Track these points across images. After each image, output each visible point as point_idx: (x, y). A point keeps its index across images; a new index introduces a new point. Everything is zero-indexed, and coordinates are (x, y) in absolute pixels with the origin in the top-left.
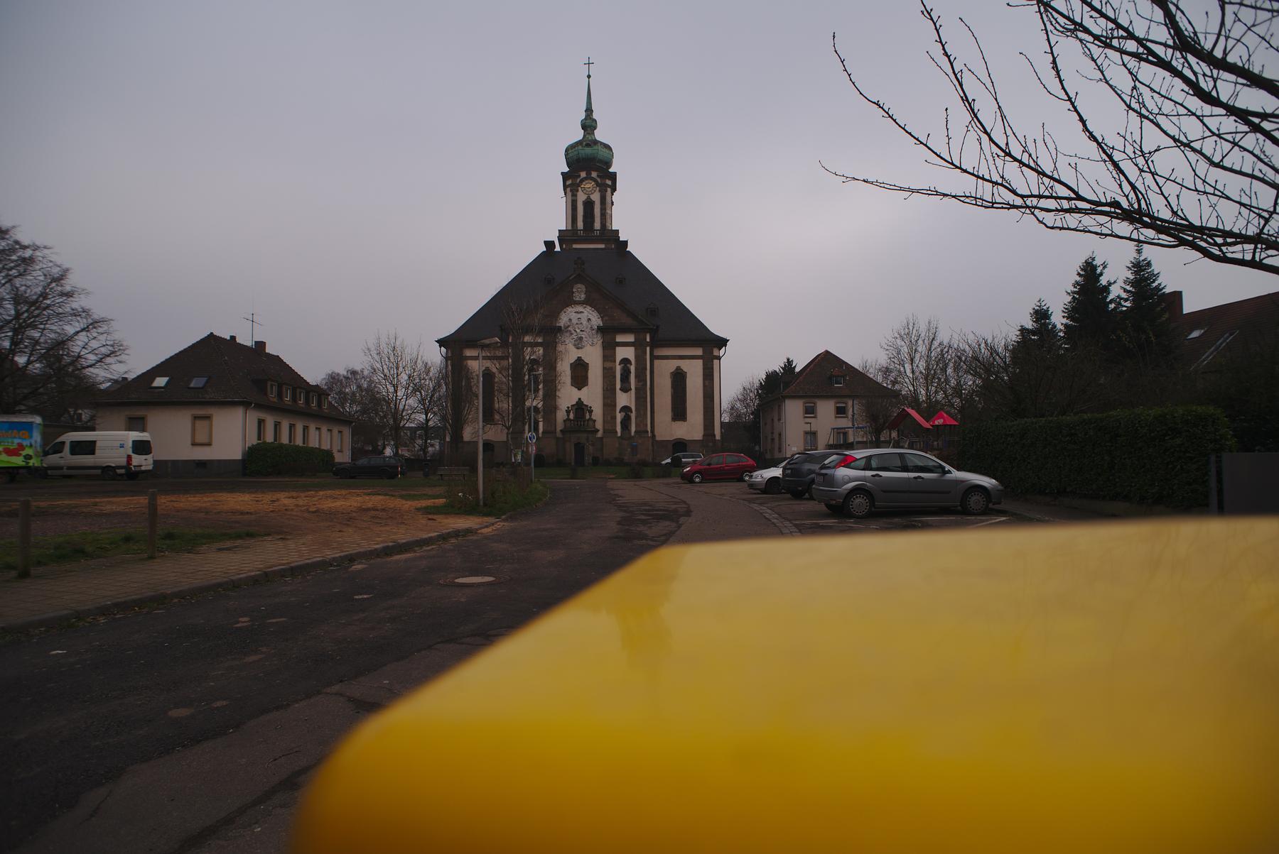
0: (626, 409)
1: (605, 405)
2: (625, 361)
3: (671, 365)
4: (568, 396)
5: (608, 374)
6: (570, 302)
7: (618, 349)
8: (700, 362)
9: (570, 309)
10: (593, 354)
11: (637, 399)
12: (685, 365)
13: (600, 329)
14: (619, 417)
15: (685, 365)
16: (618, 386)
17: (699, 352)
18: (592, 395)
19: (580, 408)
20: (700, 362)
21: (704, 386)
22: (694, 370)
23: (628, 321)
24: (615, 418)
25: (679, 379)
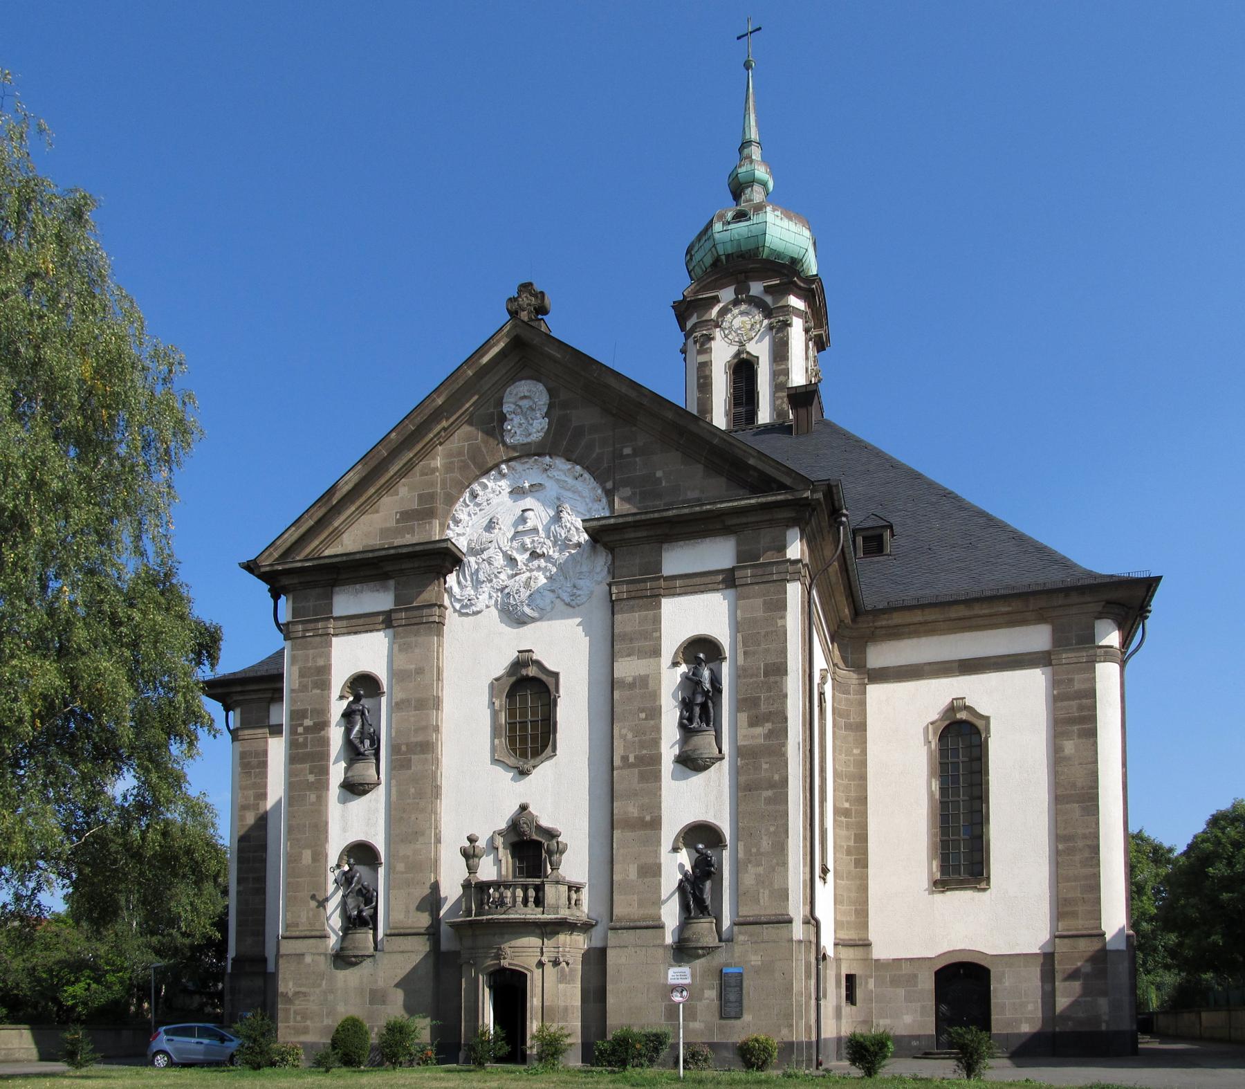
0: (701, 836)
2: (701, 650)
3: (928, 699)
4: (475, 796)
5: (619, 702)
7: (671, 607)
12: (982, 693)
14: (675, 864)
15: (982, 693)
19: (530, 847)
21: (1057, 759)
22: (1014, 708)
23: (700, 489)
24: (652, 871)
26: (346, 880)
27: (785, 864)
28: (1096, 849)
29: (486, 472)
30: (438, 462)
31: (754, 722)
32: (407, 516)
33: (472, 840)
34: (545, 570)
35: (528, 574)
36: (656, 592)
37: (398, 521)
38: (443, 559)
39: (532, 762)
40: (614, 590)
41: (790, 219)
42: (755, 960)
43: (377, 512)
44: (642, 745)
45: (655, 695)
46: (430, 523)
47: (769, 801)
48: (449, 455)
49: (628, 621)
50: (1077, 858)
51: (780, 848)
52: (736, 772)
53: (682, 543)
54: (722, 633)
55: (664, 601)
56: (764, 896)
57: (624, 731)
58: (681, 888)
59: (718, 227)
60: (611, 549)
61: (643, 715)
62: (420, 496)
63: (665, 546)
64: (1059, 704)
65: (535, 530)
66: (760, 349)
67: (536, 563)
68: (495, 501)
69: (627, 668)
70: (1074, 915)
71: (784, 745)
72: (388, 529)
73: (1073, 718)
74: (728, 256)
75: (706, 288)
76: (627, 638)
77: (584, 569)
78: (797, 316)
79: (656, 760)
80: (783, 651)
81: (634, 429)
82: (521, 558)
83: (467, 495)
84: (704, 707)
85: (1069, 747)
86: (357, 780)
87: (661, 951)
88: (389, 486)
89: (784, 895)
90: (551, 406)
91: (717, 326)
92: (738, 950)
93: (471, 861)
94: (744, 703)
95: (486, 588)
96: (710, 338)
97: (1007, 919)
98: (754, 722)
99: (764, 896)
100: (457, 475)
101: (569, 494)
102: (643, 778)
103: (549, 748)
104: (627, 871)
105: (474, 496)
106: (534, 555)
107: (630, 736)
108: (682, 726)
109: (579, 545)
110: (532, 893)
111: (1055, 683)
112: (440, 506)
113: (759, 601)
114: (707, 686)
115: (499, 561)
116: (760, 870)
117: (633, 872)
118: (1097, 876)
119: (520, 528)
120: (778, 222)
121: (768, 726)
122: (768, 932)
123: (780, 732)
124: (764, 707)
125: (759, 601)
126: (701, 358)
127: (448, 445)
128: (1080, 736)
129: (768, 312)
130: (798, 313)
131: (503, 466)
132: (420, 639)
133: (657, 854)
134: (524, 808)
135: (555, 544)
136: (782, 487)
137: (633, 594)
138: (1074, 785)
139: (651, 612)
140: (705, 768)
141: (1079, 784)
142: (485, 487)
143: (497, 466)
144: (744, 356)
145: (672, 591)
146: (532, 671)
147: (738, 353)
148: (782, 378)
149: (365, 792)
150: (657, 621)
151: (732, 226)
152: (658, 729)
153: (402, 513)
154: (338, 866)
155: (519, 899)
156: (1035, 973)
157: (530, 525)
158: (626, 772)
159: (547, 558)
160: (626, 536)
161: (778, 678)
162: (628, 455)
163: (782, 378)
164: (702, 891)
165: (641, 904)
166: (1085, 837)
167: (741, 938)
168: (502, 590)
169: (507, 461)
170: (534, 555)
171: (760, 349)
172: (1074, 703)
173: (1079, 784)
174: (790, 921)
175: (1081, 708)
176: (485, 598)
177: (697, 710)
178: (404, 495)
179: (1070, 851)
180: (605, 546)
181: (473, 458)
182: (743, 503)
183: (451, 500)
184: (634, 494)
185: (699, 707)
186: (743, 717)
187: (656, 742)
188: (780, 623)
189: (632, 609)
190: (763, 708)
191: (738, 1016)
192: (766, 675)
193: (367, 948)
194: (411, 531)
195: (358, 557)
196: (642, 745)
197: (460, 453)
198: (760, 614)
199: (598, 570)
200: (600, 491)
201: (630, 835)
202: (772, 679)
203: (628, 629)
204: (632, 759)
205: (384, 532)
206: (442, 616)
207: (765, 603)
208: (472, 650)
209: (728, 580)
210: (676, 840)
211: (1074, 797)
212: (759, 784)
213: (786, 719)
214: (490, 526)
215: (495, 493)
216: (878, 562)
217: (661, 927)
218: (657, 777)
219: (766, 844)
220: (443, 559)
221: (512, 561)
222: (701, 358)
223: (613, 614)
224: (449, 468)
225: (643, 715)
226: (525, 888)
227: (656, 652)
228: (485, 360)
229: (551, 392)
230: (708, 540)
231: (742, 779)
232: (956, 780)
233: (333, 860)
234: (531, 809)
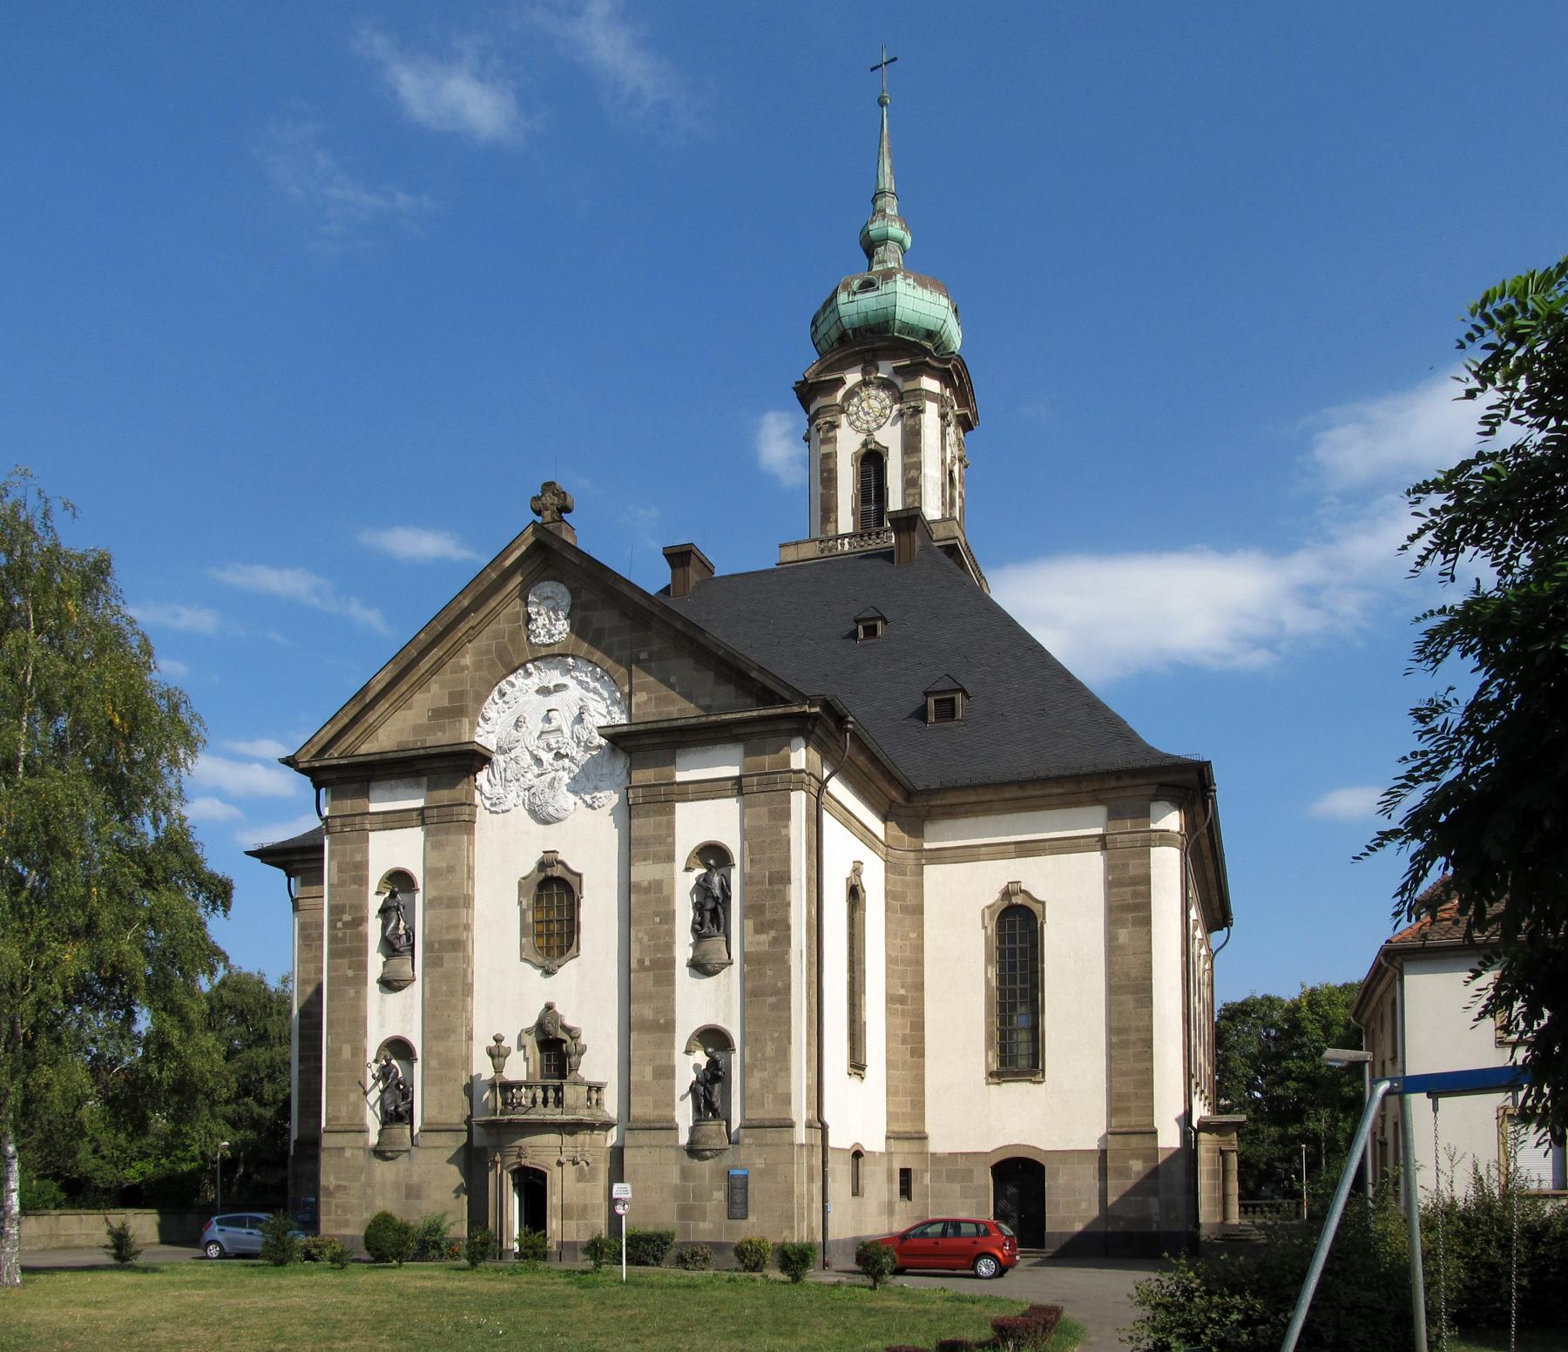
0: (712, 1038)
1: (628, 1026)
2: (712, 855)
6: (510, 661)
7: (684, 813)
8: (1094, 862)
9: (517, 679)
10: (590, 840)
11: (750, 995)
13: (618, 740)
14: (688, 1066)
16: (683, 949)
17: (1092, 822)
18: (587, 993)
19: (555, 1045)
20: (1094, 862)
21: (1112, 948)
24: (666, 1073)
25: (1017, 931)
26: (385, 1073)
27: (787, 1069)
28: (1148, 1043)
29: (514, 670)
30: (467, 660)
31: (760, 929)
32: (437, 713)
33: (498, 1039)
34: (570, 771)
35: (553, 774)
37: (430, 719)
38: (472, 760)
39: (557, 962)
40: (631, 795)
41: (924, 286)
42: (759, 1163)
43: (410, 708)
44: (657, 949)
45: (669, 900)
47: (773, 1007)
49: (644, 826)
50: (1131, 1051)
51: (783, 1054)
52: (744, 977)
54: (732, 841)
55: (680, 808)
56: (769, 1099)
57: (640, 935)
58: (693, 1090)
59: (843, 297)
60: (629, 752)
61: (657, 920)
62: (451, 695)
64: (1114, 890)
65: (559, 730)
66: (890, 437)
68: (521, 700)
69: (643, 872)
70: (1127, 1110)
71: (787, 952)
72: (421, 726)
73: (1128, 905)
74: (855, 330)
75: (830, 368)
76: (645, 842)
77: (605, 771)
78: (932, 400)
79: (670, 964)
80: (787, 860)
82: (547, 757)
83: (495, 693)
84: (714, 911)
85: (1123, 935)
86: (392, 976)
87: (673, 1152)
88: (420, 684)
89: (786, 1100)
90: (573, 607)
91: (843, 411)
92: (743, 1152)
93: (499, 1061)
94: (748, 910)
95: (514, 786)
96: (834, 426)
97: (1060, 1114)
98: (760, 929)
99: (769, 1099)
100: (485, 673)
101: (591, 695)
102: (657, 982)
103: (574, 948)
104: (643, 1073)
105: (502, 694)
107: (646, 939)
108: (694, 930)
109: (600, 747)
110: (551, 1094)
111: (1110, 868)
112: (471, 705)
113: (764, 810)
114: (717, 892)
115: (528, 760)
116: (765, 1074)
117: (648, 1074)
118: (1150, 1071)
119: (547, 727)
120: (910, 291)
121: (773, 933)
122: (771, 1135)
123: (784, 939)
124: (769, 915)
125: (764, 810)
126: (825, 449)
127: (476, 643)
128: (1134, 924)
129: (899, 397)
130: (932, 396)
131: (529, 666)
132: (452, 838)
133: (671, 1056)
134: (549, 1007)
135: (578, 745)
136: (785, 702)
138: (1128, 974)
140: (715, 973)
141: (1133, 975)
142: (513, 685)
144: (872, 446)
146: (557, 871)
147: (865, 444)
148: (913, 473)
149: (400, 989)
150: (671, 827)
151: (858, 297)
152: (671, 934)
154: (376, 1061)
155: (539, 1100)
156: (1092, 1168)
157: (554, 724)
158: (643, 975)
159: (572, 759)
161: (780, 887)
163: (913, 473)
164: (711, 1093)
165: (655, 1106)
166: (1138, 1030)
167: (747, 1141)
168: (529, 789)
169: (533, 661)
170: (559, 756)
171: (890, 437)
172: (1129, 889)
173: (1133, 975)
174: (791, 1126)
175: (1135, 895)
176: (513, 797)
177: (708, 915)
178: (433, 694)
179: (1124, 1045)
180: (623, 749)
181: (501, 657)
182: (746, 714)
183: (481, 699)
184: (650, 699)
185: (711, 912)
186: (749, 923)
187: (670, 946)
188: (784, 832)
189: (647, 815)
190: (768, 915)
191: (745, 1217)
192: (771, 883)
193: (402, 1144)
194: (442, 728)
196: (657, 949)
197: (488, 652)
198: (765, 822)
201: (646, 1037)
202: (776, 887)
203: (644, 833)
204: (647, 963)
205: (417, 729)
206: (473, 814)
207: (770, 811)
208: (502, 851)
209: (738, 787)
210: (689, 1043)
211: (1129, 988)
212: (765, 992)
213: (789, 927)
214: (518, 725)
215: (523, 688)
216: (947, 729)
217: (675, 1128)
218: (670, 980)
219: (770, 1049)
220: (472, 760)
221: (538, 761)
222: (825, 449)
224: (478, 666)
225: (657, 920)
226: (545, 1089)
227: (670, 858)
228: (508, 563)
229: (574, 593)
231: (749, 985)
232: (1012, 967)
233: (371, 1054)
234: (557, 1008)
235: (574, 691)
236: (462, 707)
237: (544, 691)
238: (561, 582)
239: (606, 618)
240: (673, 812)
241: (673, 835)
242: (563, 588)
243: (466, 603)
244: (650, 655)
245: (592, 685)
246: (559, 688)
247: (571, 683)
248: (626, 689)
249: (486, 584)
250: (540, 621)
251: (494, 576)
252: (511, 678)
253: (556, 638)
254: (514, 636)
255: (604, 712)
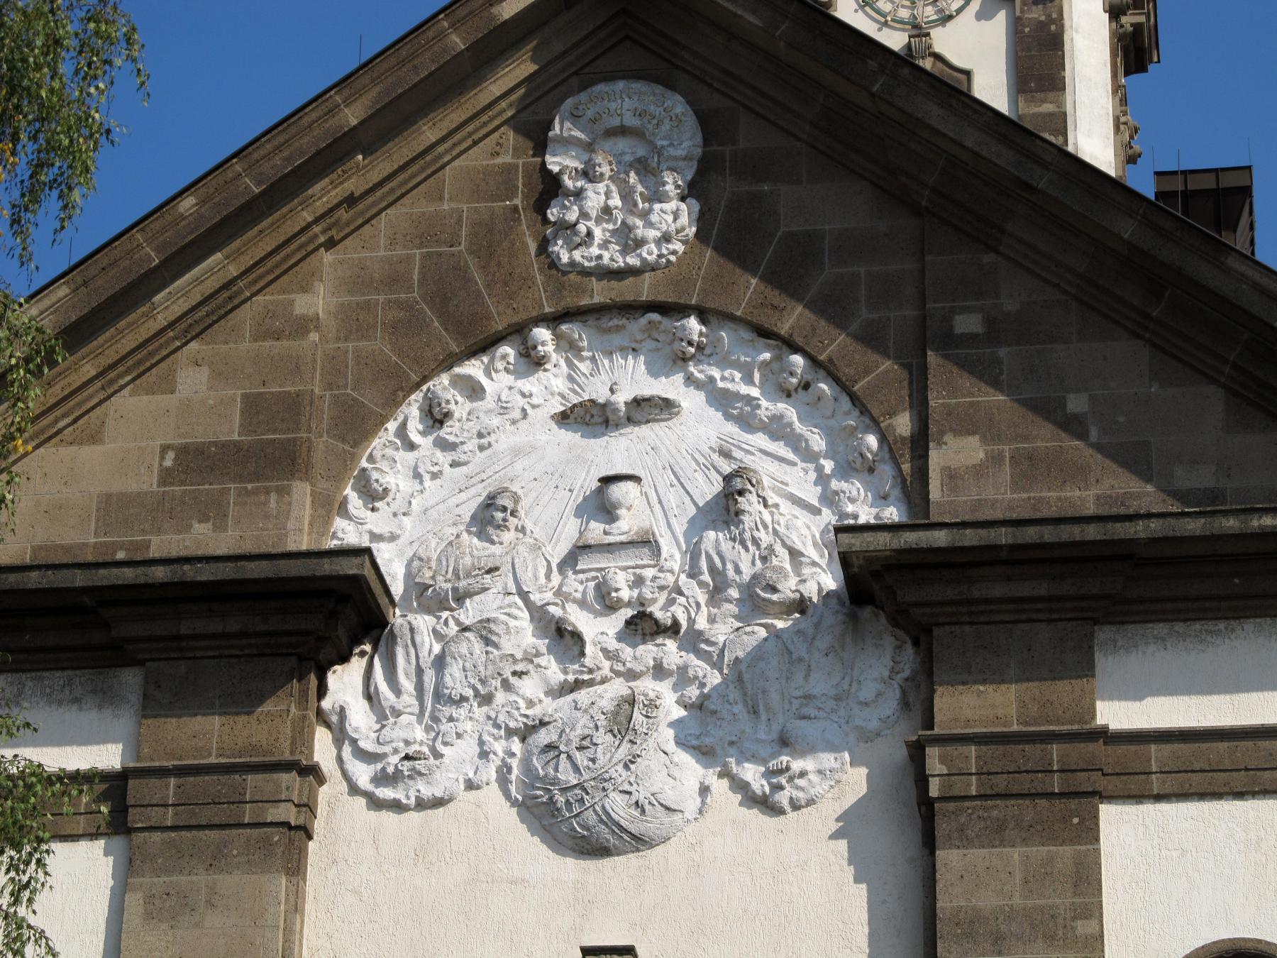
6: (488, 298)
7: (1136, 841)
9: (495, 375)
29: (484, 346)
30: (318, 301)
32: (195, 462)
34: (683, 677)
35: (618, 688)
36: (1083, 781)
37: (166, 477)
38: (337, 610)
40: (935, 761)
43: (95, 438)
46: (283, 492)
48: (359, 281)
53: (1161, 628)
55: (1111, 816)
60: (918, 632)
62: (252, 405)
63: (1103, 634)
65: (646, 542)
67: (647, 652)
68: (504, 441)
72: (126, 500)
77: (820, 684)
81: (988, 258)
82: (599, 631)
83: (412, 410)
88: (145, 363)
95: (470, 720)
100: (380, 345)
101: (761, 440)
105: (436, 417)
106: (642, 626)
109: (801, 605)
112: (322, 445)
115: (522, 635)
119: (596, 530)
127: (351, 250)
131: (542, 334)
132: (228, 882)
135: (716, 593)
137: (1001, 783)
139: (1067, 851)
142: (474, 391)
143: (518, 332)
145: (1134, 784)
150: (1086, 880)
153: (184, 452)
157: (626, 525)
159: (694, 641)
160: (977, 592)
162: (971, 339)
168: (525, 733)
169: (553, 321)
170: (642, 626)
176: (464, 754)
178: (196, 395)
183: (358, 426)
184: (995, 459)
189: (997, 834)
194: (214, 512)
195: (34, 580)
197: (394, 279)
199: (867, 692)
200: (872, 441)
203: (987, 901)
205: (114, 507)
206: (309, 807)
214: (490, 515)
220: (337, 610)
221: (564, 639)
223: (929, 843)
224: (354, 322)
229: (705, 120)
230: (1249, 625)
235: (698, 426)
236: (290, 441)
237: (589, 417)
238: (671, 86)
239: (825, 207)
240: (1090, 832)
241: (1093, 910)
242: (677, 104)
243: (352, 116)
244: (990, 322)
245: (768, 408)
246: (648, 409)
247: (691, 401)
248: (903, 424)
249: (427, 65)
250: (595, 198)
251: (457, 42)
252: (473, 368)
253: (650, 253)
254: (490, 241)
255: (806, 506)
